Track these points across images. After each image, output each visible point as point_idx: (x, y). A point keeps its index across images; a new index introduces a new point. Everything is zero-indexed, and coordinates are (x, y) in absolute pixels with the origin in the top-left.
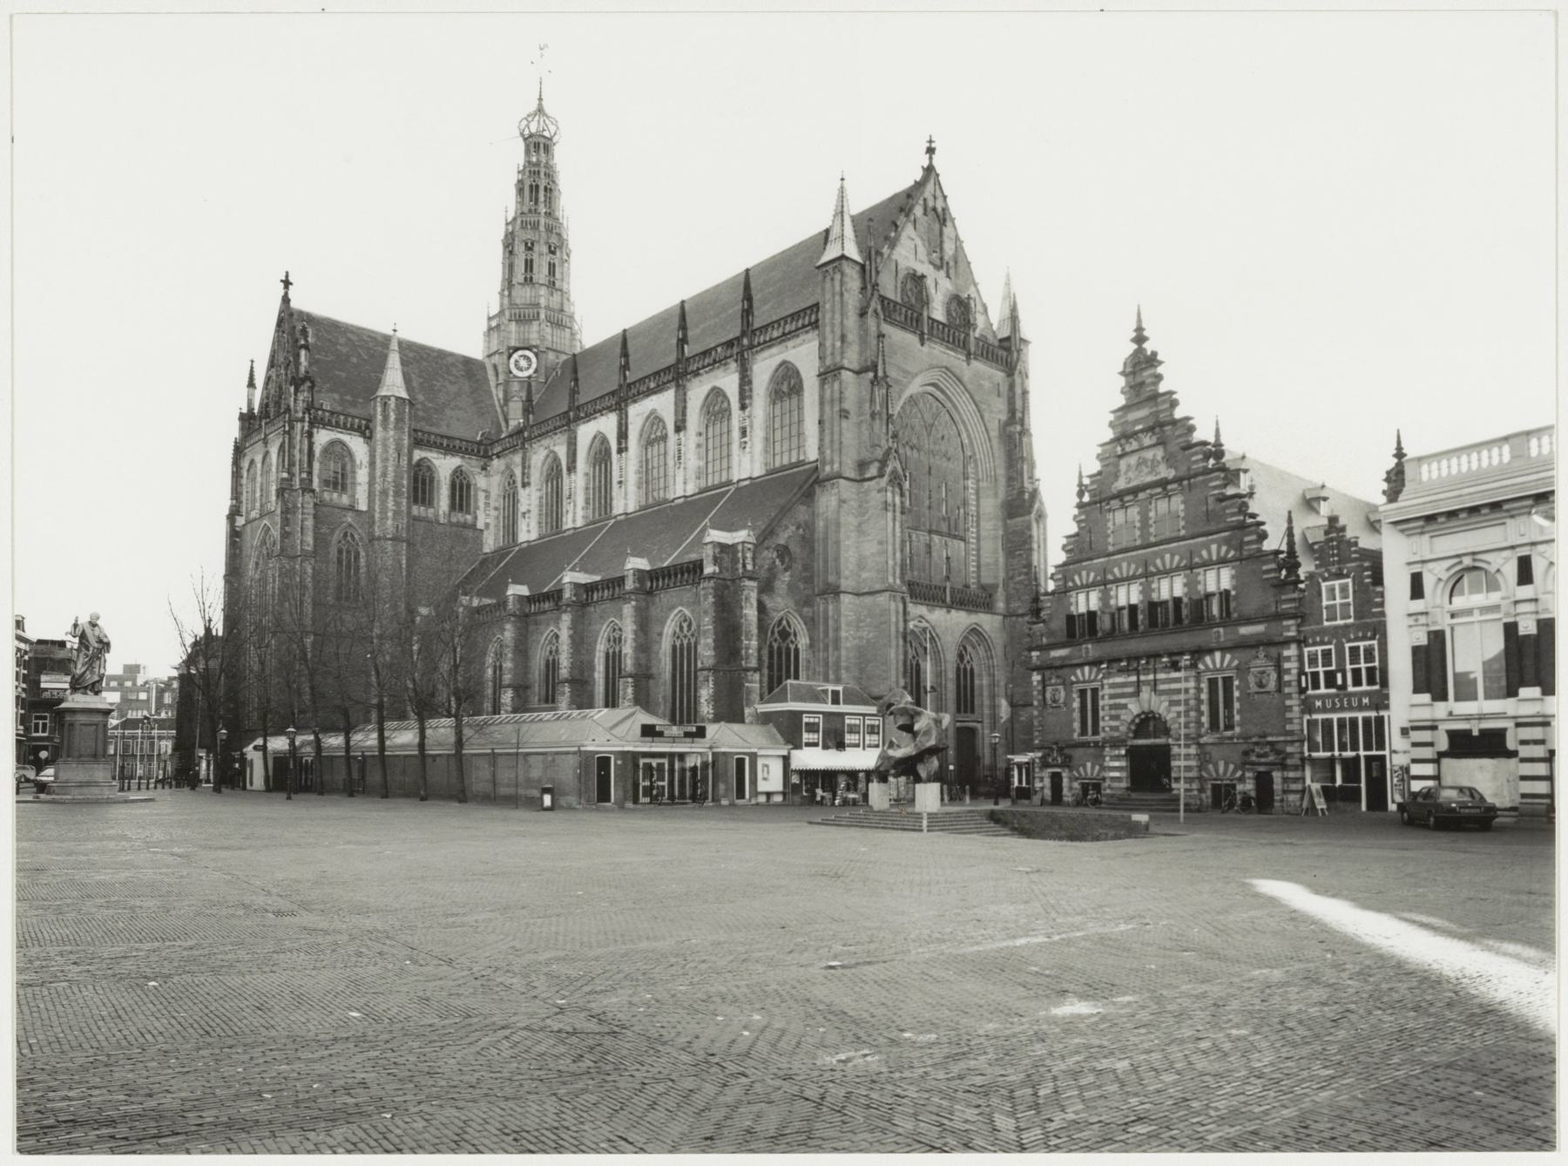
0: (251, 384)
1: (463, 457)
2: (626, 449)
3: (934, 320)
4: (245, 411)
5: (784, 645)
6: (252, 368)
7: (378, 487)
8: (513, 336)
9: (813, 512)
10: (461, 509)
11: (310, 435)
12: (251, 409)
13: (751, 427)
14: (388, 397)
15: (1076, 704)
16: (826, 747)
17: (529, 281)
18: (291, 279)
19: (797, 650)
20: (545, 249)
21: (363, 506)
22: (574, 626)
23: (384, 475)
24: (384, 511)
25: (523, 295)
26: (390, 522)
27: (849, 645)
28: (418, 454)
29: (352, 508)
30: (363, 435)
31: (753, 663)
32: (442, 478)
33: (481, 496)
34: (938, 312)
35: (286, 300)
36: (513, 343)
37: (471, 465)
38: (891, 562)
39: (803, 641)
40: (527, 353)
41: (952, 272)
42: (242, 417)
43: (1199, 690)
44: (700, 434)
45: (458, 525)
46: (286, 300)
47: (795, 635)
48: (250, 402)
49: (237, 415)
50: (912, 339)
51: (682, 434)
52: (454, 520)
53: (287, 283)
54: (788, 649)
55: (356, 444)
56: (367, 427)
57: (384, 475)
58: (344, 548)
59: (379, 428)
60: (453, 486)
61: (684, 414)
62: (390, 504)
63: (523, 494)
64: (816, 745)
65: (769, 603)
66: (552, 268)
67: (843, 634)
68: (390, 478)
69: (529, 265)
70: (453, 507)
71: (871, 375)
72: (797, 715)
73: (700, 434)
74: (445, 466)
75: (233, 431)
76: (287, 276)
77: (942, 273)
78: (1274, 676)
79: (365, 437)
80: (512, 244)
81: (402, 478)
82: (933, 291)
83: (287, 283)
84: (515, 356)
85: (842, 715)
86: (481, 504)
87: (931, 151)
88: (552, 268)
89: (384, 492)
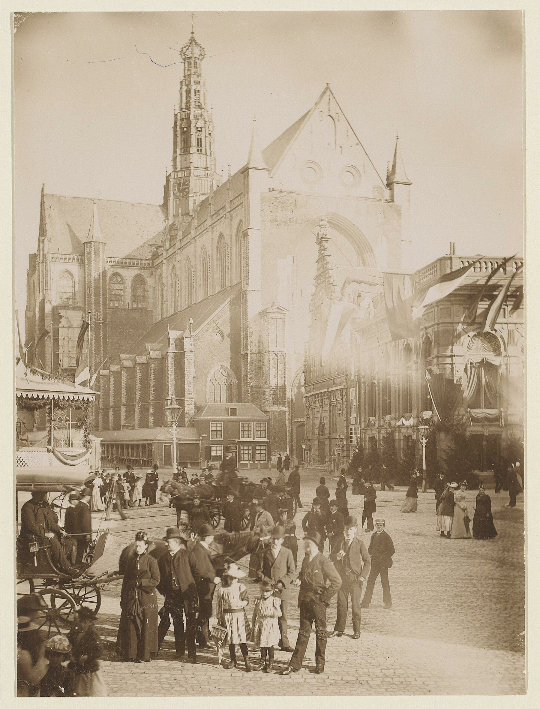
66: (199, 141)
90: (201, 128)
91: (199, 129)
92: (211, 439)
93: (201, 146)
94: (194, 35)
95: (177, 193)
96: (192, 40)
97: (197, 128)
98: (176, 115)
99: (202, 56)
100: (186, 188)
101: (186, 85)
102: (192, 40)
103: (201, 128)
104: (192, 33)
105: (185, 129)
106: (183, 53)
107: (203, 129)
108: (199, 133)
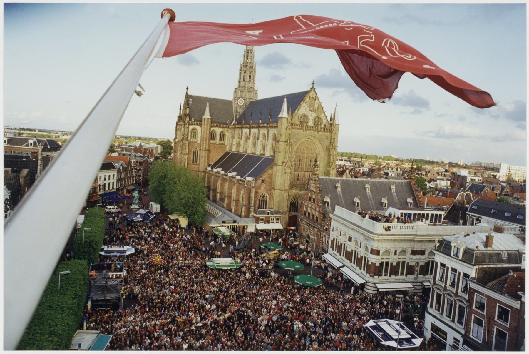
0: (180, 109)
7: (202, 138)
8: (239, 95)
11: (188, 128)
12: (180, 115)
16: (265, 223)
17: (244, 80)
20: (249, 72)
21: (199, 142)
22: (229, 185)
23: (204, 135)
24: (203, 143)
25: (242, 84)
26: (204, 146)
29: (197, 142)
30: (200, 125)
31: (253, 205)
33: (227, 137)
34: (311, 123)
36: (239, 97)
38: (286, 185)
39: (268, 198)
40: (242, 99)
41: (316, 111)
48: (180, 113)
50: (302, 131)
52: (220, 143)
53: (187, 89)
54: (264, 200)
57: (204, 135)
60: (220, 135)
62: (205, 142)
64: (263, 223)
65: (259, 191)
66: (250, 77)
67: (275, 198)
68: (205, 136)
69: (244, 76)
71: (286, 143)
72: (259, 218)
77: (313, 112)
82: (310, 117)
83: (187, 89)
84: (239, 100)
85: (270, 217)
86: (227, 139)
88: (250, 77)
89: (203, 140)
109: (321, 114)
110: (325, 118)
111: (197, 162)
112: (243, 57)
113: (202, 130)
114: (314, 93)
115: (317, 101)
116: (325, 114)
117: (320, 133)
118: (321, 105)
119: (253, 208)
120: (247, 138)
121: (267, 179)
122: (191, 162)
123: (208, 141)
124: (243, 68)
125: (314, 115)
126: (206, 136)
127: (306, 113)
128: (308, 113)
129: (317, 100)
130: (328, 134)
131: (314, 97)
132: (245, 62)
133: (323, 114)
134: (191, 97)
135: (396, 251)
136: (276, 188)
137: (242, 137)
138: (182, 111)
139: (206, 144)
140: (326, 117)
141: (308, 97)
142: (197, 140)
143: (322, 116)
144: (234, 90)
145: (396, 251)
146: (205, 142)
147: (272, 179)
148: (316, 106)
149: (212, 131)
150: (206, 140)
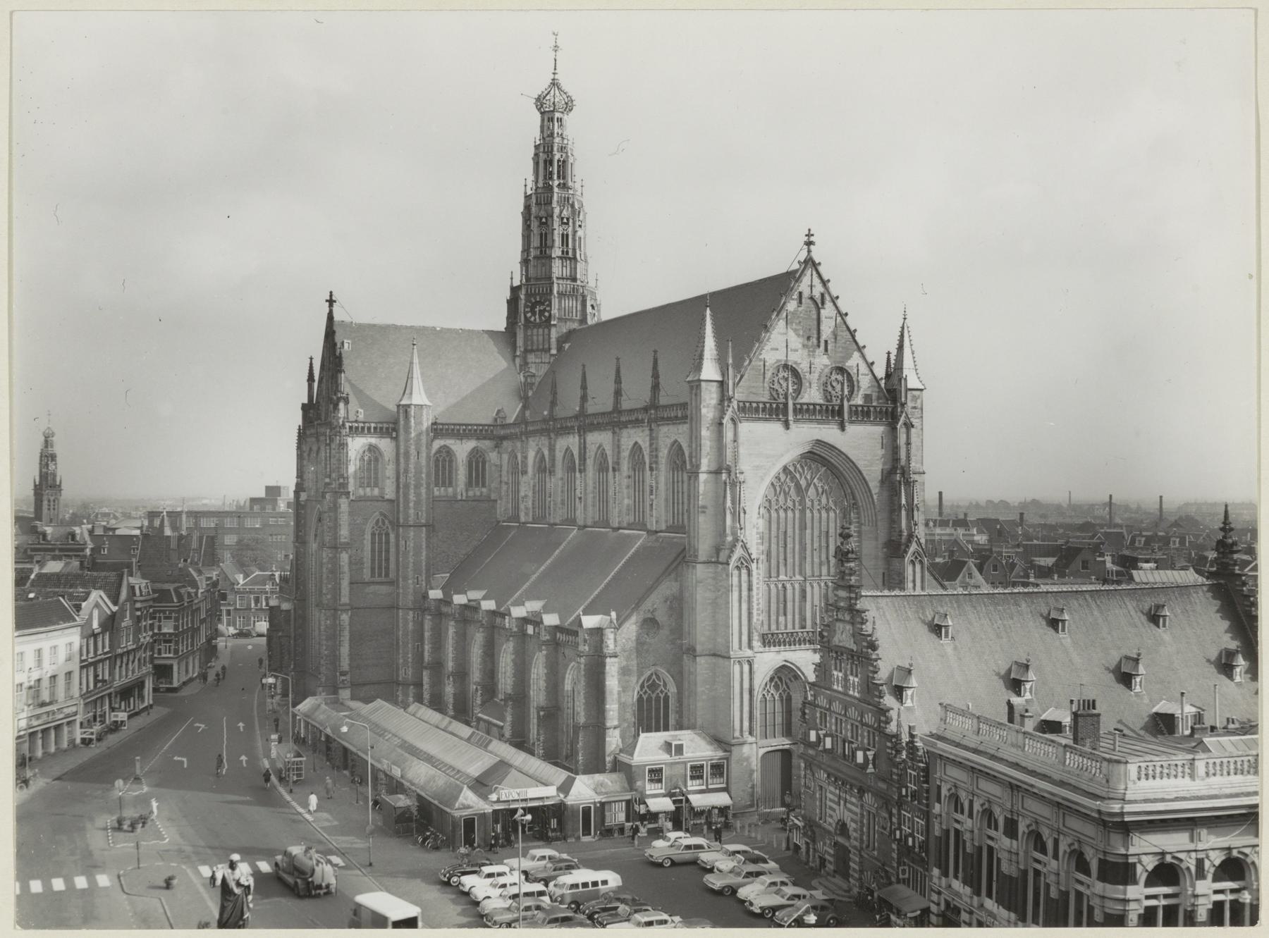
1: (478, 439)
2: (585, 470)
3: (801, 404)
4: (306, 401)
5: (654, 696)
6: (311, 364)
9: (681, 586)
10: (477, 485)
11: (343, 445)
13: (657, 488)
14: (409, 406)
15: (818, 796)
18: (334, 298)
19: (666, 698)
23: (406, 471)
24: (407, 501)
27: (704, 697)
28: (437, 444)
32: (460, 460)
35: (330, 317)
37: (486, 444)
42: (304, 407)
43: (862, 815)
44: (629, 477)
45: (476, 500)
46: (330, 317)
47: (665, 685)
49: (300, 406)
51: (617, 473)
52: (471, 493)
53: (331, 302)
54: (658, 698)
55: (385, 445)
56: (394, 430)
58: (377, 532)
59: (402, 431)
61: (619, 458)
63: (523, 479)
67: (700, 689)
70: (469, 484)
73: (629, 477)
74: (462, 449)
75: (298, 419)
76: (331, 296)
78: (889, 824)
79: (392, 438)
80: (530, 219)
81: (421, 473)
83: (331, 302)
87: (809, 243)
88: (565, 238)
90: (568, 219)
91: (565, 220)
92: (648, 793)
93: (567, 246)
94: (556, 77)
95: (531, 317)
96: (554, 84)
97: (562, 219)
98: (527, 197)
99: (569, 107)
100: (545, 310)
101: (544, 152)
102: (554, 84)
103: (568, 219)
104: (554, 74)
105: (544, 220)
106: (540, 101)
107: (571, 221)
108: (564, 226)
109: (849, 356)
110: (863, 368)
111: (387, 575)
112: (531, 164)
113: (398, 447)
114: (816, 281)
115: (828, 311)
116: (863, 356)
117: (851, 429)
118: (845, 323)
119: (617, 732)
120: (571, 468)
121: (661, 617)
122: (367, 575)
123: (423, 491)
124: (534, 209)
125: (823, 361)
126: (418, 472)
127: (793, 358)
128: (799, 358)
129: (829, 305)
130: (878, 430)
131: (817, 294)
132: (540, 184)
133: (856, 354)
134: (349, 327)
135: (1200, 863)
136: (699, 648)
137: (553, 465)
138: (316, 385)
139: (418, 503)
140: (870, 365)
141: (795, 296)
142: (382, 489)
143: (854, 362)
144: (508, 295)
145: (1200, 863)
146: (412, 497)
147: (681, 616)
148: (827, 329)
149: (439, 451)
150: (417, 487)
